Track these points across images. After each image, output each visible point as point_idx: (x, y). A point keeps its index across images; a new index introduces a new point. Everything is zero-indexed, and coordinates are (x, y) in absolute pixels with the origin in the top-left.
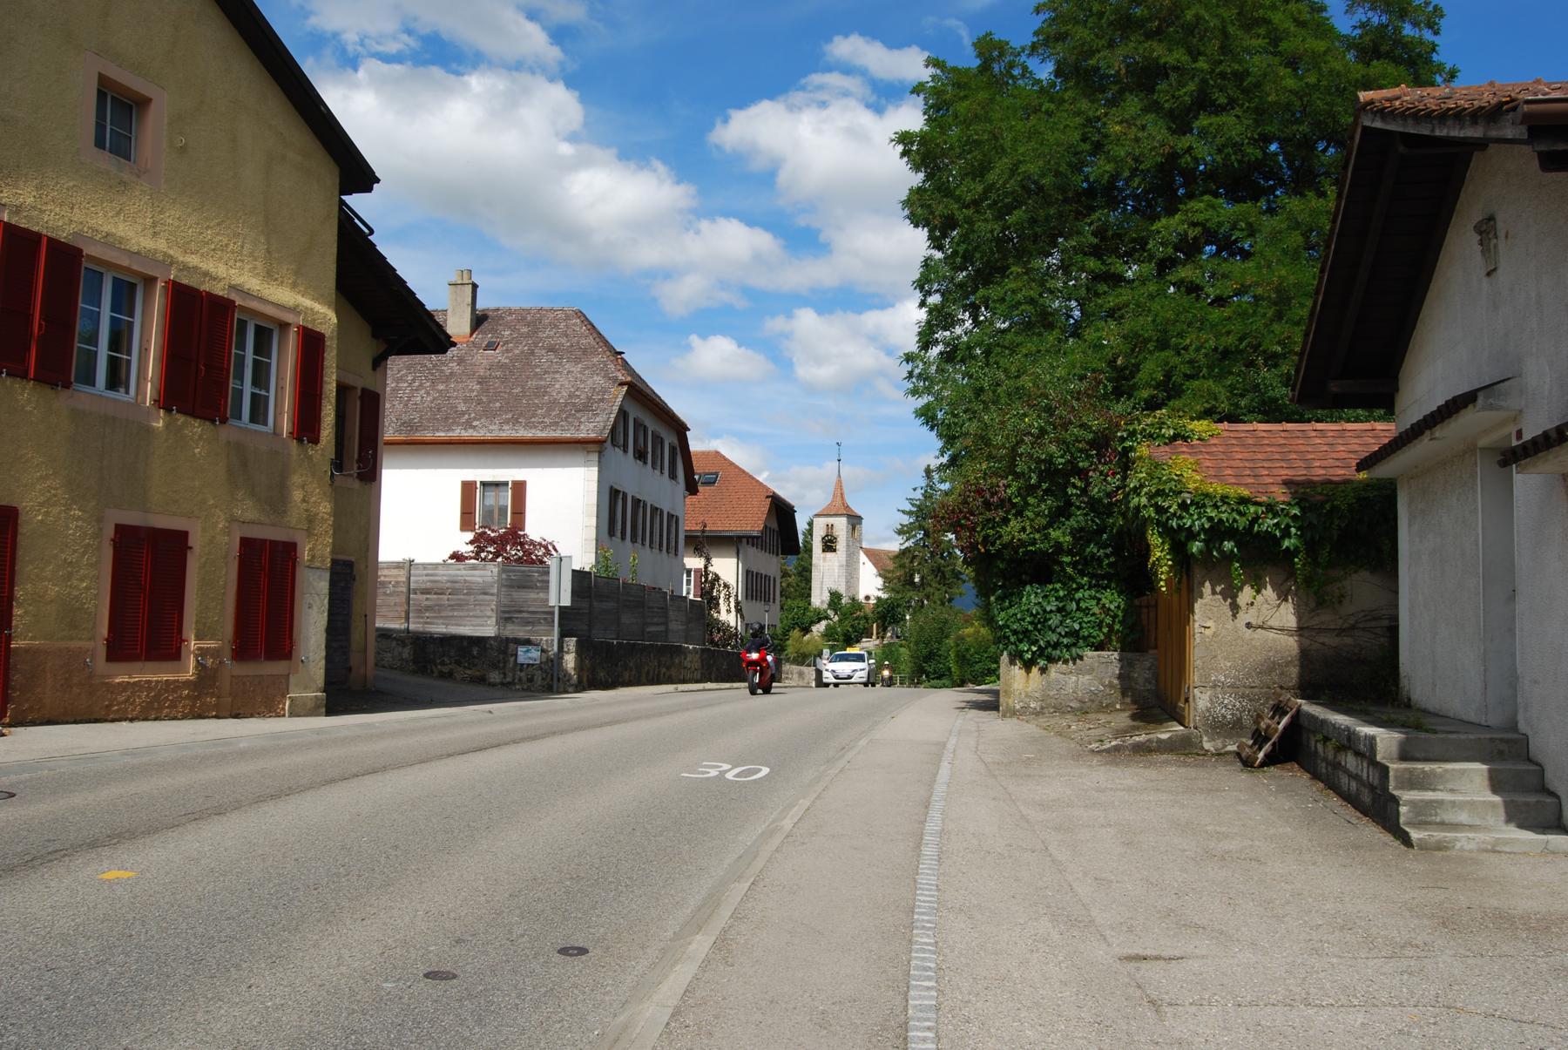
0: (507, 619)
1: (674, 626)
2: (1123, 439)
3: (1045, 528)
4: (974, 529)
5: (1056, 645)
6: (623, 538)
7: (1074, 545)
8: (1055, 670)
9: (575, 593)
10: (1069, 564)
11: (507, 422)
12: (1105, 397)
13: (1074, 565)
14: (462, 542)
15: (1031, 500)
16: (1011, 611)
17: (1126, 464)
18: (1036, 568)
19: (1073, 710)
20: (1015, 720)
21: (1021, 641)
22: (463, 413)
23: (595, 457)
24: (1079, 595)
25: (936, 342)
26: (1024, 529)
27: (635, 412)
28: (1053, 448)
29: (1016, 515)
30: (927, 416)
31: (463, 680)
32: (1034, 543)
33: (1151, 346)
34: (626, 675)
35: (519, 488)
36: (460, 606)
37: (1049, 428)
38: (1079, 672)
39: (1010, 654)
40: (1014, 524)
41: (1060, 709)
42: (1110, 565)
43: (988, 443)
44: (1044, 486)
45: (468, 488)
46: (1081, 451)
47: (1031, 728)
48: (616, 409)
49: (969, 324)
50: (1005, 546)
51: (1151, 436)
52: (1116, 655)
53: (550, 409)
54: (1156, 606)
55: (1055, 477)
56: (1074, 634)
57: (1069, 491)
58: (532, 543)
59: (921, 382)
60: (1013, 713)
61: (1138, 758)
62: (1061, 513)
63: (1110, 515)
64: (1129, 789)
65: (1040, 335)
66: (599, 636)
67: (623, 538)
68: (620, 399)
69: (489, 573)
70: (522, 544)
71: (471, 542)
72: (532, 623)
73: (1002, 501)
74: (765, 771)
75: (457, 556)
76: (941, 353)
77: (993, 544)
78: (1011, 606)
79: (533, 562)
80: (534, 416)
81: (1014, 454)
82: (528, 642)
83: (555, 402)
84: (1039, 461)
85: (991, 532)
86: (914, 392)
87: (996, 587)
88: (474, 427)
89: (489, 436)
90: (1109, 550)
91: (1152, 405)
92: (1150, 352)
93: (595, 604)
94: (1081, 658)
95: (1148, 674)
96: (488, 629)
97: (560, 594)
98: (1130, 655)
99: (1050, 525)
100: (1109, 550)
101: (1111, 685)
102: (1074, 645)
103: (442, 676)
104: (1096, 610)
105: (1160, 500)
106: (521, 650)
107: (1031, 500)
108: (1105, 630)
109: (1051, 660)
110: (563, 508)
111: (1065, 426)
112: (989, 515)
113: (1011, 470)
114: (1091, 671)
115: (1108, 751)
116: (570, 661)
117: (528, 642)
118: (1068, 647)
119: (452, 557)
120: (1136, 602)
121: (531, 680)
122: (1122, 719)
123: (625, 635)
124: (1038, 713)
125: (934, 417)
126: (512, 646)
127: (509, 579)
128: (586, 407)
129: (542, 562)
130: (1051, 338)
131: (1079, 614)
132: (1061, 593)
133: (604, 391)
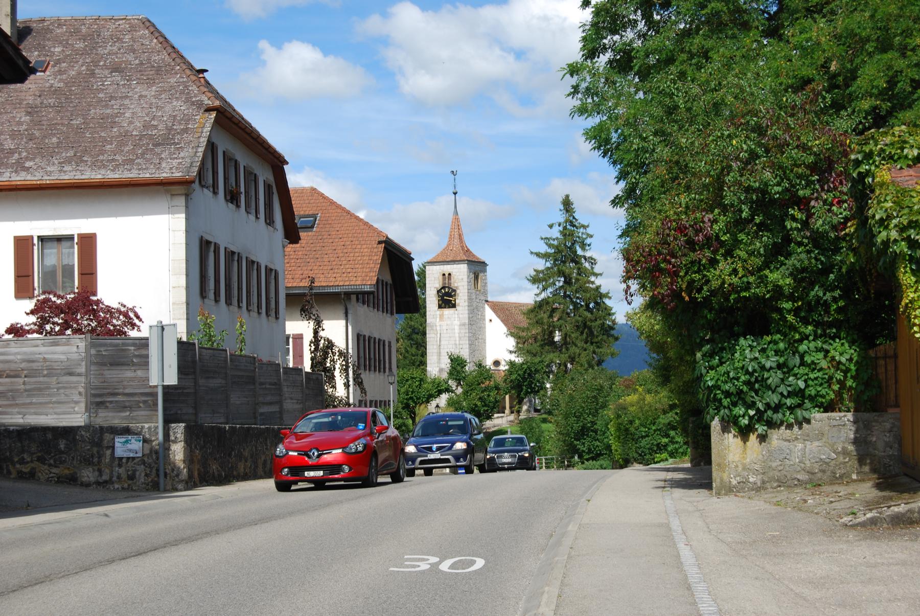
0: (100, 404)
1: (289, 405)
2: (858, 163)
3: (760, 269)
4: (676, 274)
5: (777, 408)
6: (217, 300)
7: (795, 289)
8: (777, 437)
9: (183, 370)
10: (789, 312)
11: (68, 161)
12: (824, 111)
13: (796, 312)
14: (21, 312)
15: (742, 236)
16: (722, 369)
17: (862, 192)
18: (753, 317)
19: (801, 483)
20: (732, 497)
21: (735, 404)
22: (11, 152)
23: (181, 201)
24: (803, 348)
25: (604, 49)
26: (735, 272)
27: (225, 144)
28: (767, 175)
29: (725, 256)
30: (600, 139)
31: (48, 480)
32: (748, 286)
33: (870, 47)
34: (241, 467)
35: (88, 243)
36: (39, 390)
37: (760, 151)
38: (807, 438)
39: (722, 420)
40: (724, 266)
41: (784, 483)
42: (839, 310)
43: (685, 169)
44: (758, 220)
45: (22, 245)
46: (800, 177)
47: (759, 504)
48: (204, 141)
49: (641, 25)
50: (713, 293)
51: (891, 157)
52: (850, 416)
53: (121, 144)
54: (896, 356)
55: (770, 209)
56: (800, 393)
57: (789, 224)
58: (109, 310)
59: (590, 99)
60: (729, 490)
61: (899, 531)
62: (777, 252)
63: (837, 250)
64: (904, 563)
65: (734, 37)
66: (208, 420)
67: (217, 300)
68: (208, 129)
69: (73, 348)
70: (95, 312)
71: (32, 312)
72: (130, 408)
73: (708, 238)
74: (480, 563)
75: (16, 330)
76: (610, 62)
77: (699, 290)
78: (721, 363)
79: (110, 333)
80: (102, 152)
81: (719, 184)
82: (127, 431)
83: (127, 134)
84: (748, 190)
85: (697, 276)
86: (582, 110)
87: (703, 342)
88: (27, 169)
89: (47, 180)
90: (837, 293)
91: (880, 120)
92: (870, 55)
93: (202, 382)
94: (808, 421)
95: (888, 438)
96: (76, 417)
97: (164, 371)
98: (866, 415)
99: (766, 265)
100: (837, 293)
101: (845, 452)
102: (799, 406)
103: (21, 476)
104: (824, 364)
105: (912, 233)
106: (119, 441)
107: (742, 236)
108: (836, 387)
109: (771, 424)
110: (144, 265)
111: (782, 147)
112: (693, 256)
113: (717, 202)
114: (820, 436)
115: (863, 525)
116: (178, 452)
117: (127, 431)
118: (791, 409)
119: (9, 331)
120: (872, 353)
121: (132, 477)
122: (867, 490)
123: (232, 421)
124: (759, 489)
125: (607, 141)
126: (107, 436)
127: (99, 355)
128: (167, 140)
129: (122, 333)
130: (748, 40)
131: (803, 370)
132: (782, 345)
133: (188, 119)
